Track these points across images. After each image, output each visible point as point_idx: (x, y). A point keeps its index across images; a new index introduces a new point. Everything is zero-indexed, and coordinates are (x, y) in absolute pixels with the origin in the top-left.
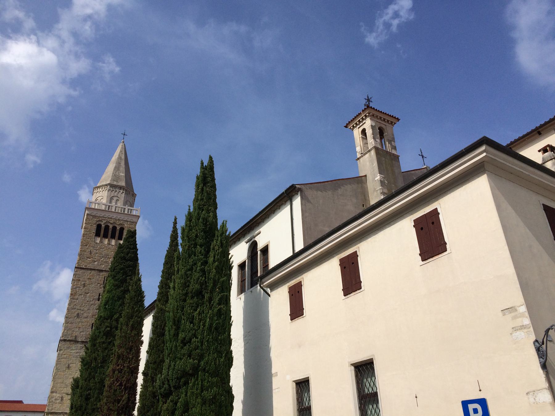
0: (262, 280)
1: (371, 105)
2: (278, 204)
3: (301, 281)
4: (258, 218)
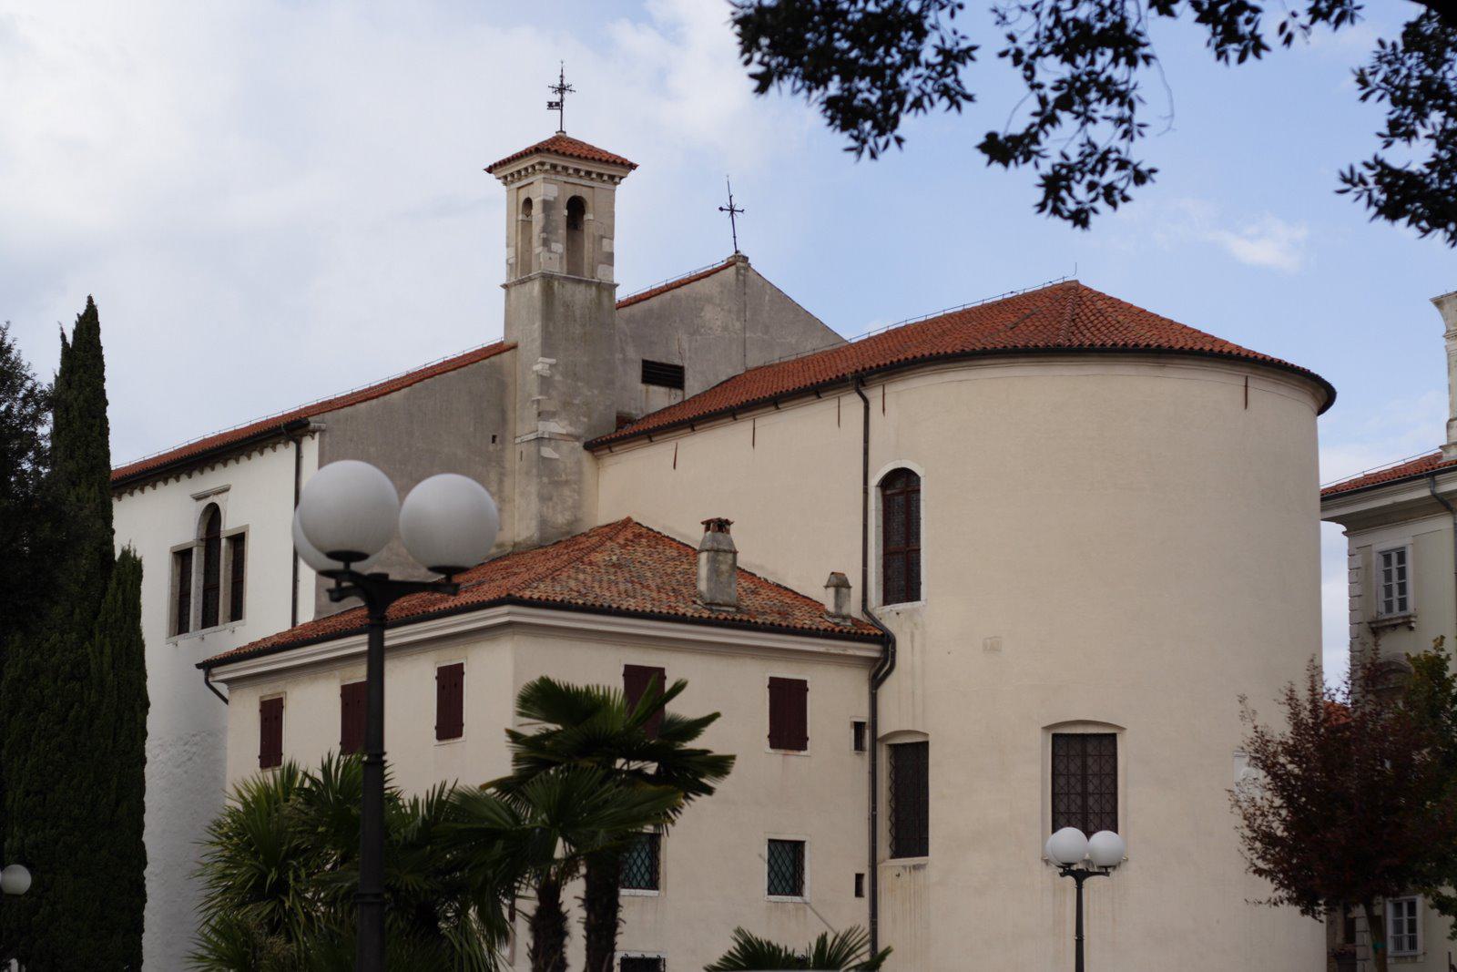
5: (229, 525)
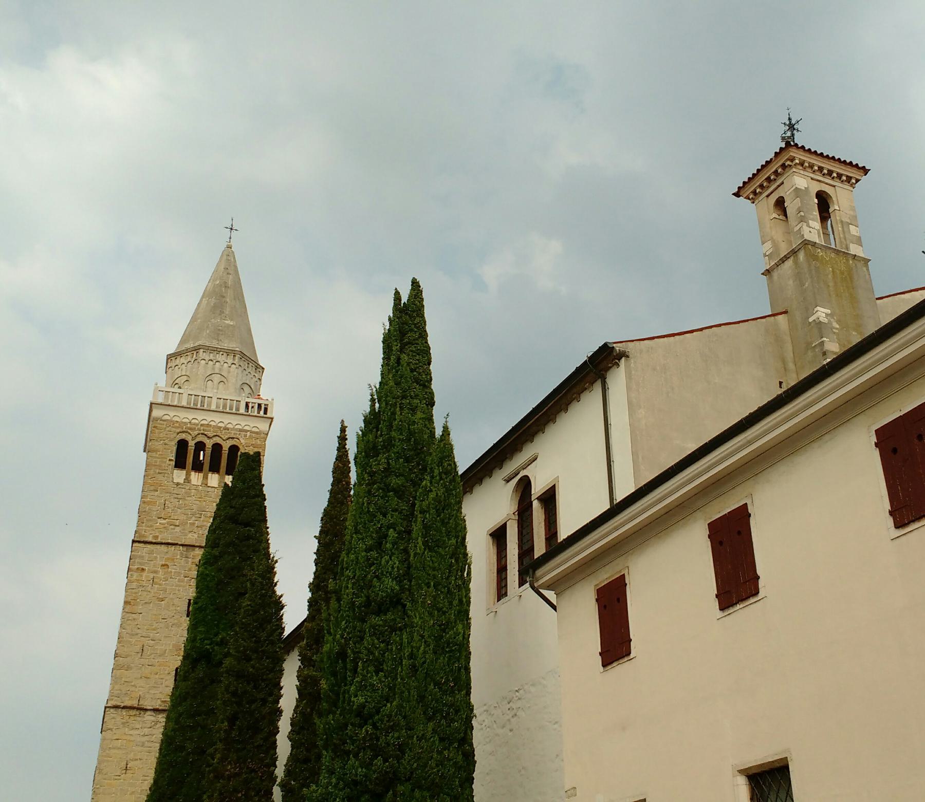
0: (536, 572)
1: (799, 140)
2: (575, 390)
3: (624, 574)
4: (525, 427)
5: (538, 489)
